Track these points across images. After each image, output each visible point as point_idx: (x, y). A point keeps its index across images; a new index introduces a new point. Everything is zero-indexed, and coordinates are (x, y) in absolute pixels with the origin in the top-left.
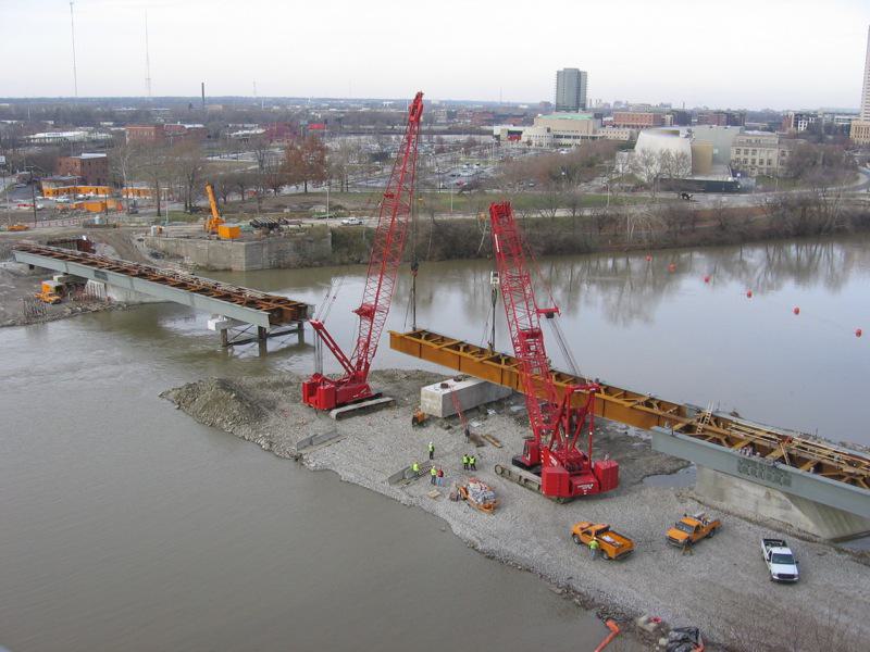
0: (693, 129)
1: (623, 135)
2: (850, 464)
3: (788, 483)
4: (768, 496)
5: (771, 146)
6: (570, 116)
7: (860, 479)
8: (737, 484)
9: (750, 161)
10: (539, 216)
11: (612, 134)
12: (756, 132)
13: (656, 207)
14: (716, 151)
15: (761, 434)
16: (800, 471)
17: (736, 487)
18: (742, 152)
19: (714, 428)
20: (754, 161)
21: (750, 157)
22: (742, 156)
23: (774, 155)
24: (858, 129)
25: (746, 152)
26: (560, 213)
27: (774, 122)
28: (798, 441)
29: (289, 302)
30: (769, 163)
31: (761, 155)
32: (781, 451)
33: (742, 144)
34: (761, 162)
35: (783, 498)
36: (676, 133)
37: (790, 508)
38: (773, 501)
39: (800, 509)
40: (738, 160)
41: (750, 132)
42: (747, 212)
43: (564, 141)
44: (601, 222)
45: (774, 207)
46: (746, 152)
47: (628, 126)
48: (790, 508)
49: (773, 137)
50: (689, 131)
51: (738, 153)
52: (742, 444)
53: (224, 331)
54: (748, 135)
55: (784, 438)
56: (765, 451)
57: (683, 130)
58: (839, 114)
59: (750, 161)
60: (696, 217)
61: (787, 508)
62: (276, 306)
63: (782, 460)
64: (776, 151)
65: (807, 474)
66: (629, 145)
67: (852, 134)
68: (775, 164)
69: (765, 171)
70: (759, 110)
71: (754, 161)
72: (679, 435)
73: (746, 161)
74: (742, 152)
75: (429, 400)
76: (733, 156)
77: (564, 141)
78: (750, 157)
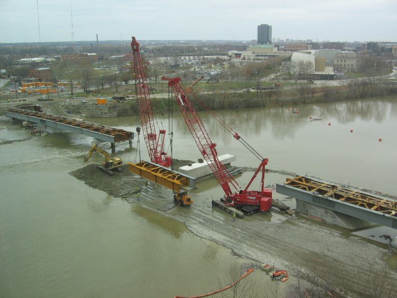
0: (317, 51)
2: (362, 197)
3: (334, 206)
4: (326, 212)
5: (354, 58)
7: (365, 204)
8: (313, 208)
9: (343, 65)
10: (241, 91)
12: (347, 52)
13: (295, 87)
14: (328, 61)
15: (324, 185)
16: (338, 201)
17: (312, 209)
19: (304, 183)
20: (345, 65)
21: (343, 63)
22: (340, 63)
23: (354, 62)
25: (341, 61)
28: (340, 188)
29: (124, 131)
30: (352, 65)
31: (347, 63)
32: (331, 192)
33: (340, 57)
34: (348, 66)
35: (333, 213)
36: (310, 53)
37: (336, 218)
38: (329, 214)
41: (344, 52)
44: (270, 95)
46: (341, 61)
48: (336, 218)
50: (316, 52)
51: (338, 61)
52: (315, 189)
54: (343, 53)
55: (334, 187)
56: (325, 192)
57: (313, 52)
59: (343, 65)
61: (335, 218)
62: (118, 133)
63: (331, 196)
64: (355, 61)
65: (342, 202)
66: (289, 59)
68: (355, 66)
71: (345, 65)
72: (288, 186)
73: (341, 65)
76: (336, 63)
78: (343, 63)
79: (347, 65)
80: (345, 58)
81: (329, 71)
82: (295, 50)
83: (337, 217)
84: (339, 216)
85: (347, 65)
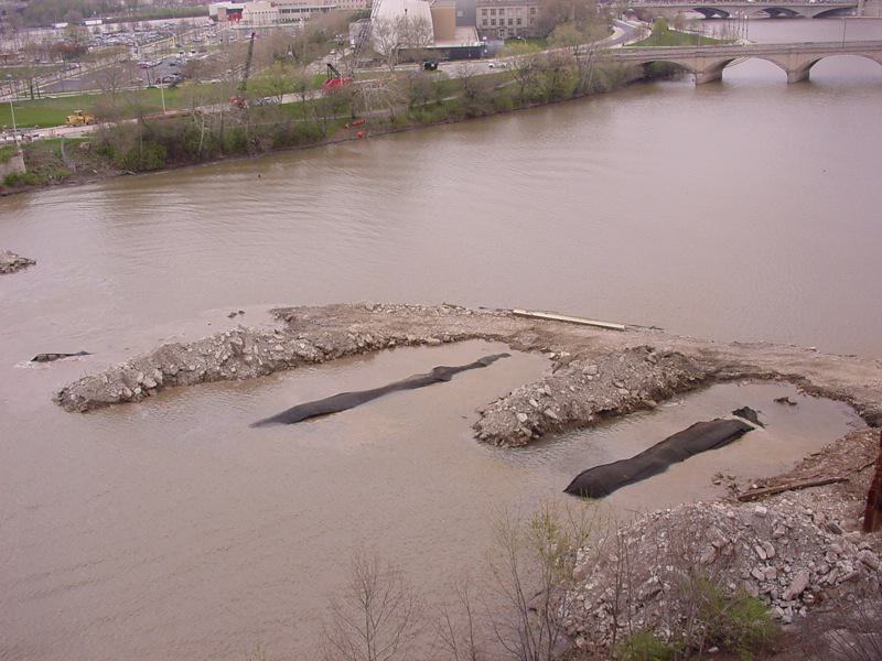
14: (460, 14)
18: (489, 12)
20: (502, 22)
21: (498, 17)
22: (489, 17)
25: (493, 13)
26: (287, 99)
31: (506, 18)
34: (510, 22)
42: (496, 80)
45: (524, 71)
46: (493, 13)
60: (442, 88)
69: (515, 32)
71: (502, 22)
73: (493, 23)
77: (291, 16)
78: (498, 17)
79: (506, 22)
81: (467, 38)
85: (506, 22)
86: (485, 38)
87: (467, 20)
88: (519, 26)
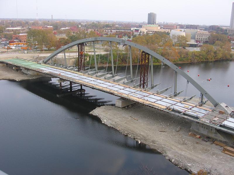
0: (185, 30)
1: (167, 31)
6: (152, 25)
11: (163, 30)
12: (202, 31)
14: (192, 36)
18: (199, 36)
20: (202, 39)
21: (201, 37)
22: (199, 37)
24: (229, 30)
25: (200, 36)
27: (206, 28)
30: (206, 39)
31: (203, 37)
36: (181, 31)
39: (220, 134)
40: (198, 38)
43: (150, 32)
46: (200, 36)
47: (167, 29)
49: (206, 32)
50: (184, 30)
53: (61, 83)
54: (201, 32)
57: (183, 30)
58: (224, 26)
64: (208, 36)
66: (168, 34)
67: (228, 32)
68: (207, 39)
70: (202, 25)
71: (202, 39)
73: (200, 39)
74: (199, 36)
75: (118, 103)
77: (150, 32)
78: (201, 37)
80: (202, 35)
81: (193, 42)
82: (172, 29)
83: (218, 133)
84: (218, 133)
86: (198, 42)
87: (193, 38)
88: (206, 40)
